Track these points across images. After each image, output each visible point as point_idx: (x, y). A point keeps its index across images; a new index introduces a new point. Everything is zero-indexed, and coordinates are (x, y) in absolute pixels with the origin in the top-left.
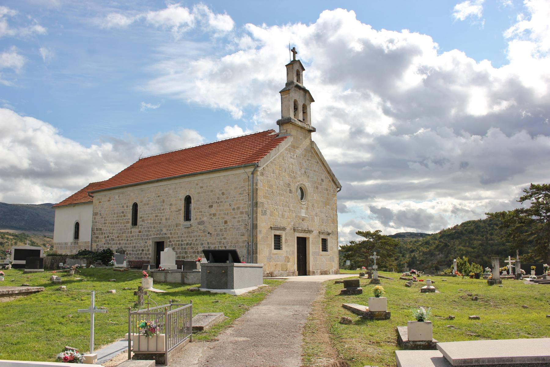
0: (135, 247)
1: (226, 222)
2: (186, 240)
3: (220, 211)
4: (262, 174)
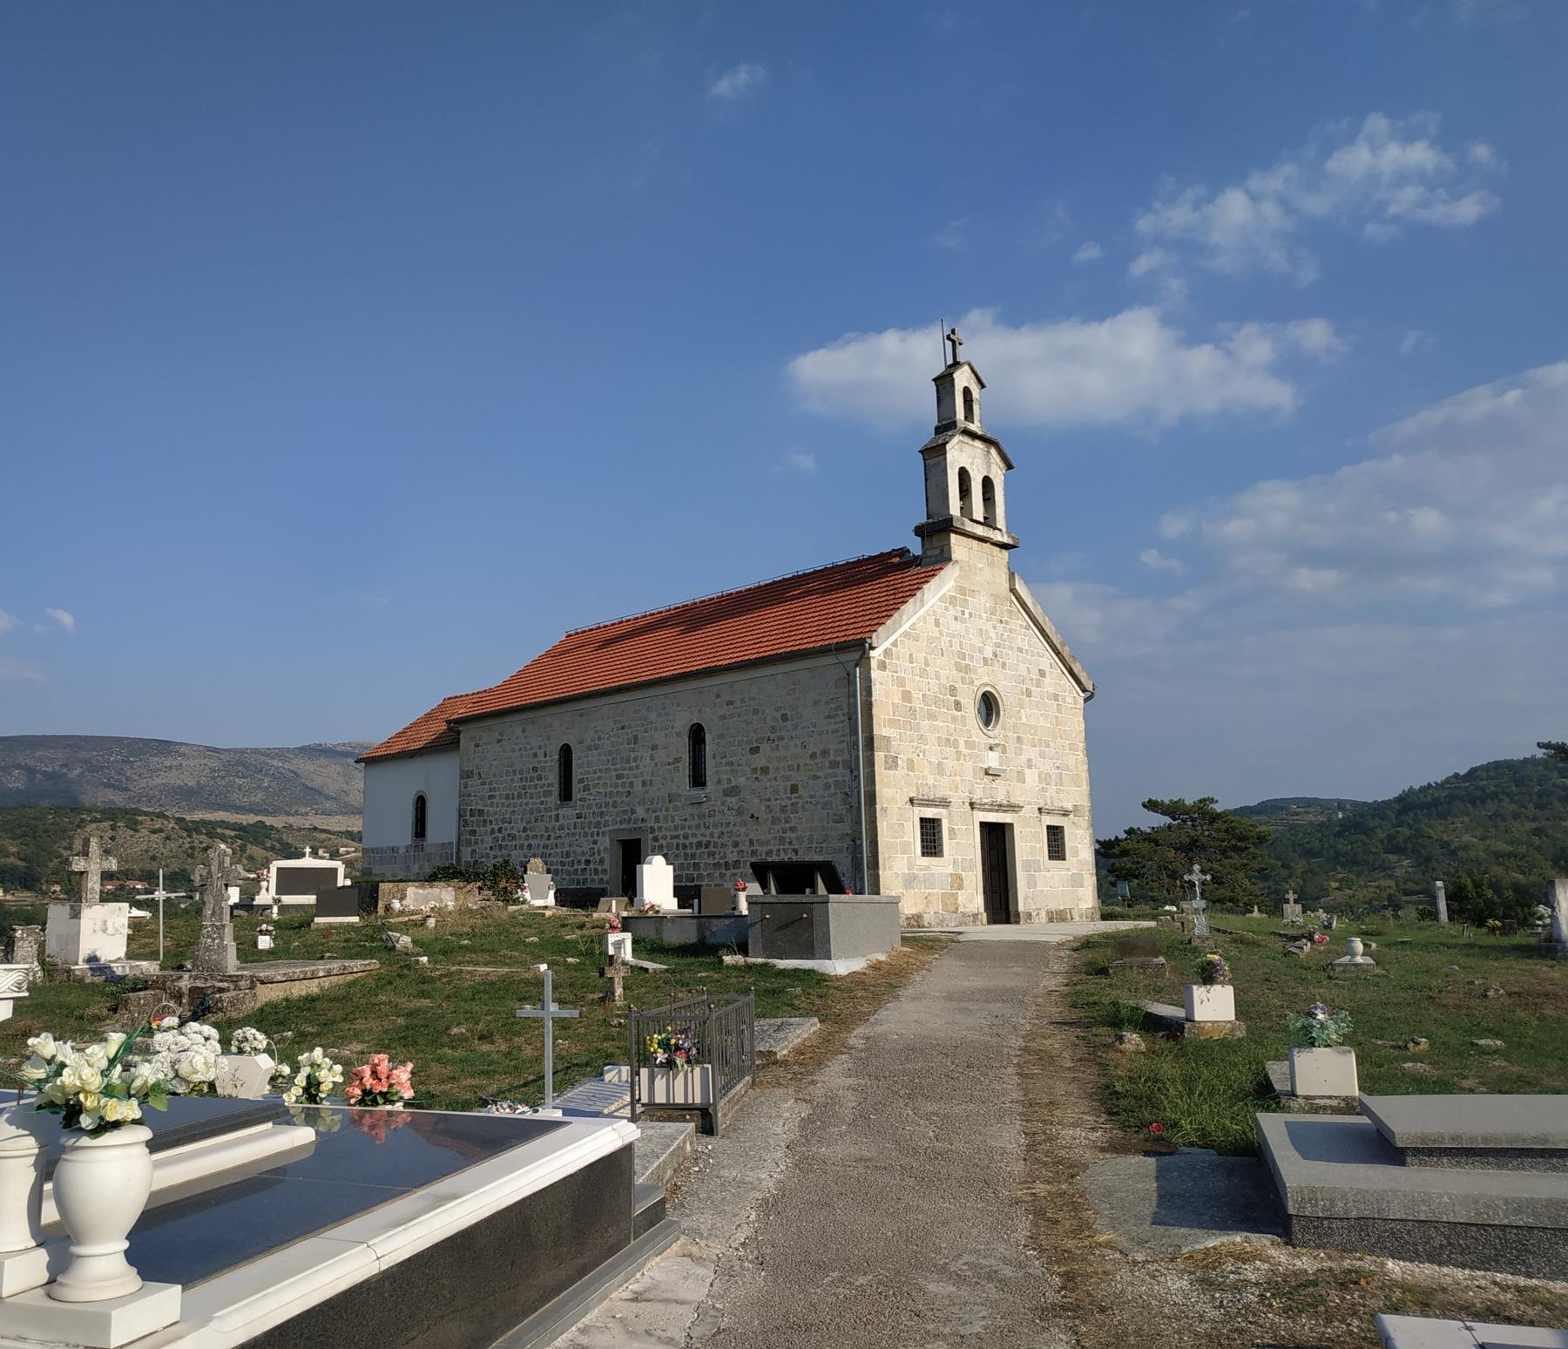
0: (568, 855)
1: (794, 789)
2: (694, 835)
3: (779, 760)
4: (882, 666)
